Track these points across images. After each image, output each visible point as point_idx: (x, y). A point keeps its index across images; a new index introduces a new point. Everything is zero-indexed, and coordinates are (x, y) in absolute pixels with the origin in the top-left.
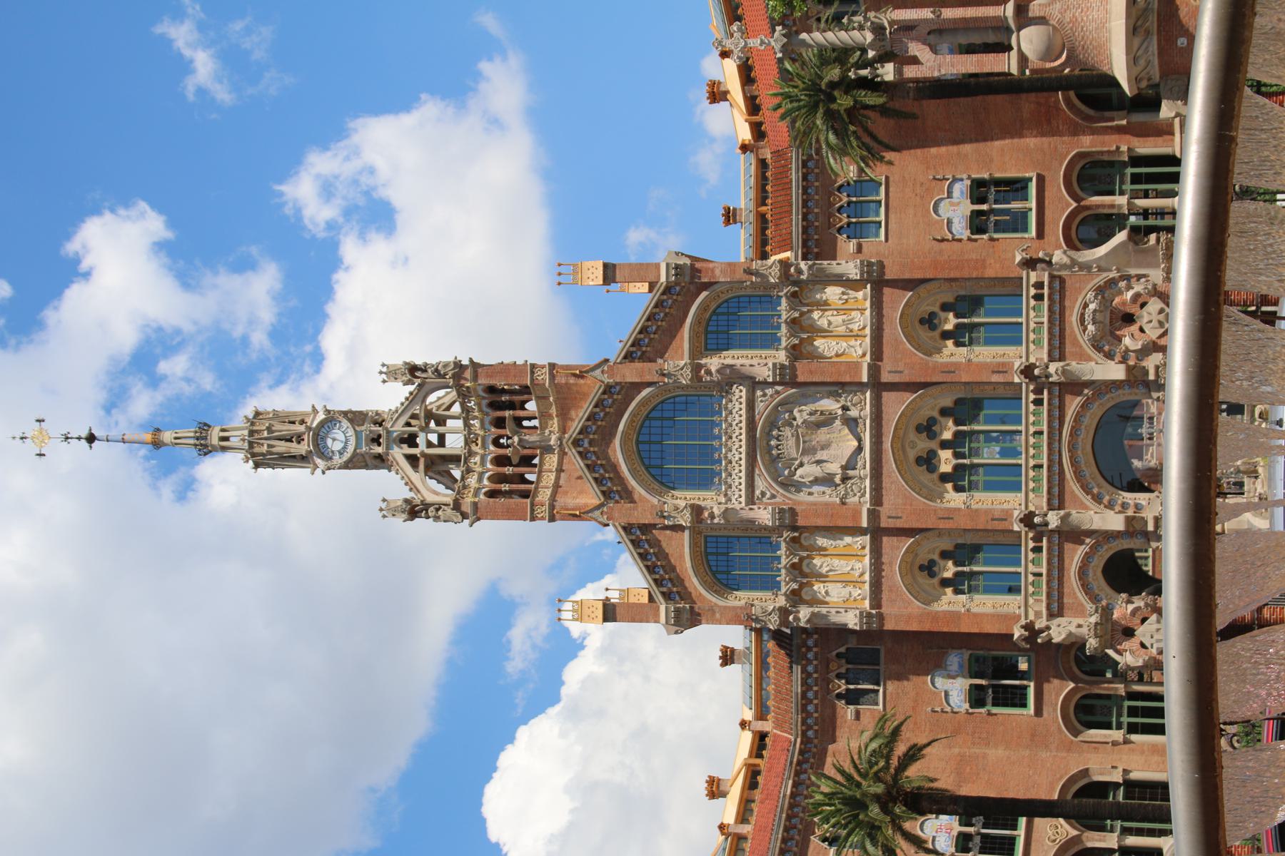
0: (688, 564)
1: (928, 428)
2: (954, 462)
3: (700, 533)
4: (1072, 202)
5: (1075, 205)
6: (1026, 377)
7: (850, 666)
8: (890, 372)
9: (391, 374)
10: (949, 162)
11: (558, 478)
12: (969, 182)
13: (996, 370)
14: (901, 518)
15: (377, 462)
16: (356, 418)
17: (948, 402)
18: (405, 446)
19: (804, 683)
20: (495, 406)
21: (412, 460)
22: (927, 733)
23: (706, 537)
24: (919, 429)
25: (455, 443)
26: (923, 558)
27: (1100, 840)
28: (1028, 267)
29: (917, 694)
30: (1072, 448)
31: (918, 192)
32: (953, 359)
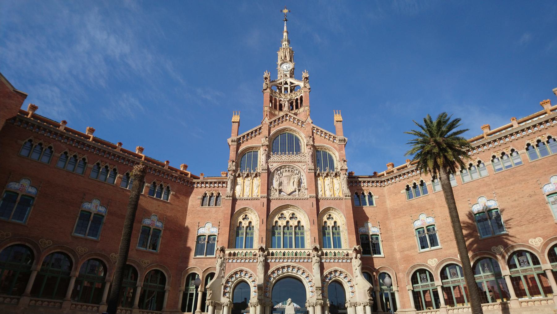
1: (293, 217)
3: (259, 149)
7: (215, 197)
8: (313, 203)
10: (384, 227)
13: (315, 238)
14: (263, 207)
17: (302, 223)
18: (285, 82)
20: (297, 99)
22: (191, 222)
23: (257, 151)
24: (293, 214)
26: (249, 216)
28: (354, 250)
29: (204, 218)
31: (372, 217)
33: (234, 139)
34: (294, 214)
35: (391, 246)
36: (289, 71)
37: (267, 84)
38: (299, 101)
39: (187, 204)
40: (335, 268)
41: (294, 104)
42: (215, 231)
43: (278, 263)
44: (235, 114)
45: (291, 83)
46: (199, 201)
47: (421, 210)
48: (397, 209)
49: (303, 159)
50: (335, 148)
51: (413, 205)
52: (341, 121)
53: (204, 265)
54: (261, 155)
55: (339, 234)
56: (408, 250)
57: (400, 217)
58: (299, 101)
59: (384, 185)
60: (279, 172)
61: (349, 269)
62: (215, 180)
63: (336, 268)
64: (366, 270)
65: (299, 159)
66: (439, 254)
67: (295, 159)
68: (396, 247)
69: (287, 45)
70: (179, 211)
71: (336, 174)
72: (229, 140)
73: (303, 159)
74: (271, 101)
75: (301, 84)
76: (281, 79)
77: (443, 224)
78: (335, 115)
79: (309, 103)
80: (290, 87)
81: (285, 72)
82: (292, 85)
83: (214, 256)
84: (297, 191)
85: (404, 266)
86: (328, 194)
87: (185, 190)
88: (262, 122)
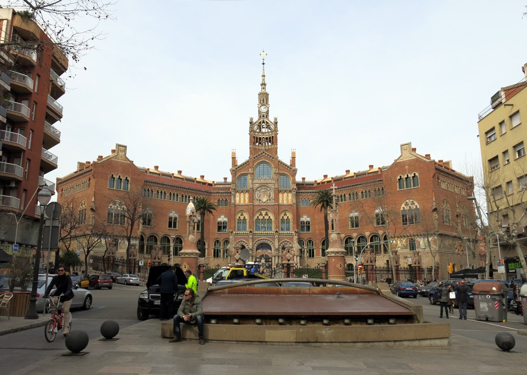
0: (242, 173)
1: (266, 214)
2: (261, 219)
9: (276, 119)
11: (257, 149)
15: (260, 116)
16: (267, 112)
17: (271, 218)
19: (222, 193)
20: (270, 137)
21: (260, 123)
24: (266, 213)
25: (263, 130)
26: (244, 214)
30: (264, 239)
58: (271, 140)
60: (259, 189)
68: (317, 228)
71: (290, 191)
81: (263, 114)
84: (269, 200)
86: (285, 202)
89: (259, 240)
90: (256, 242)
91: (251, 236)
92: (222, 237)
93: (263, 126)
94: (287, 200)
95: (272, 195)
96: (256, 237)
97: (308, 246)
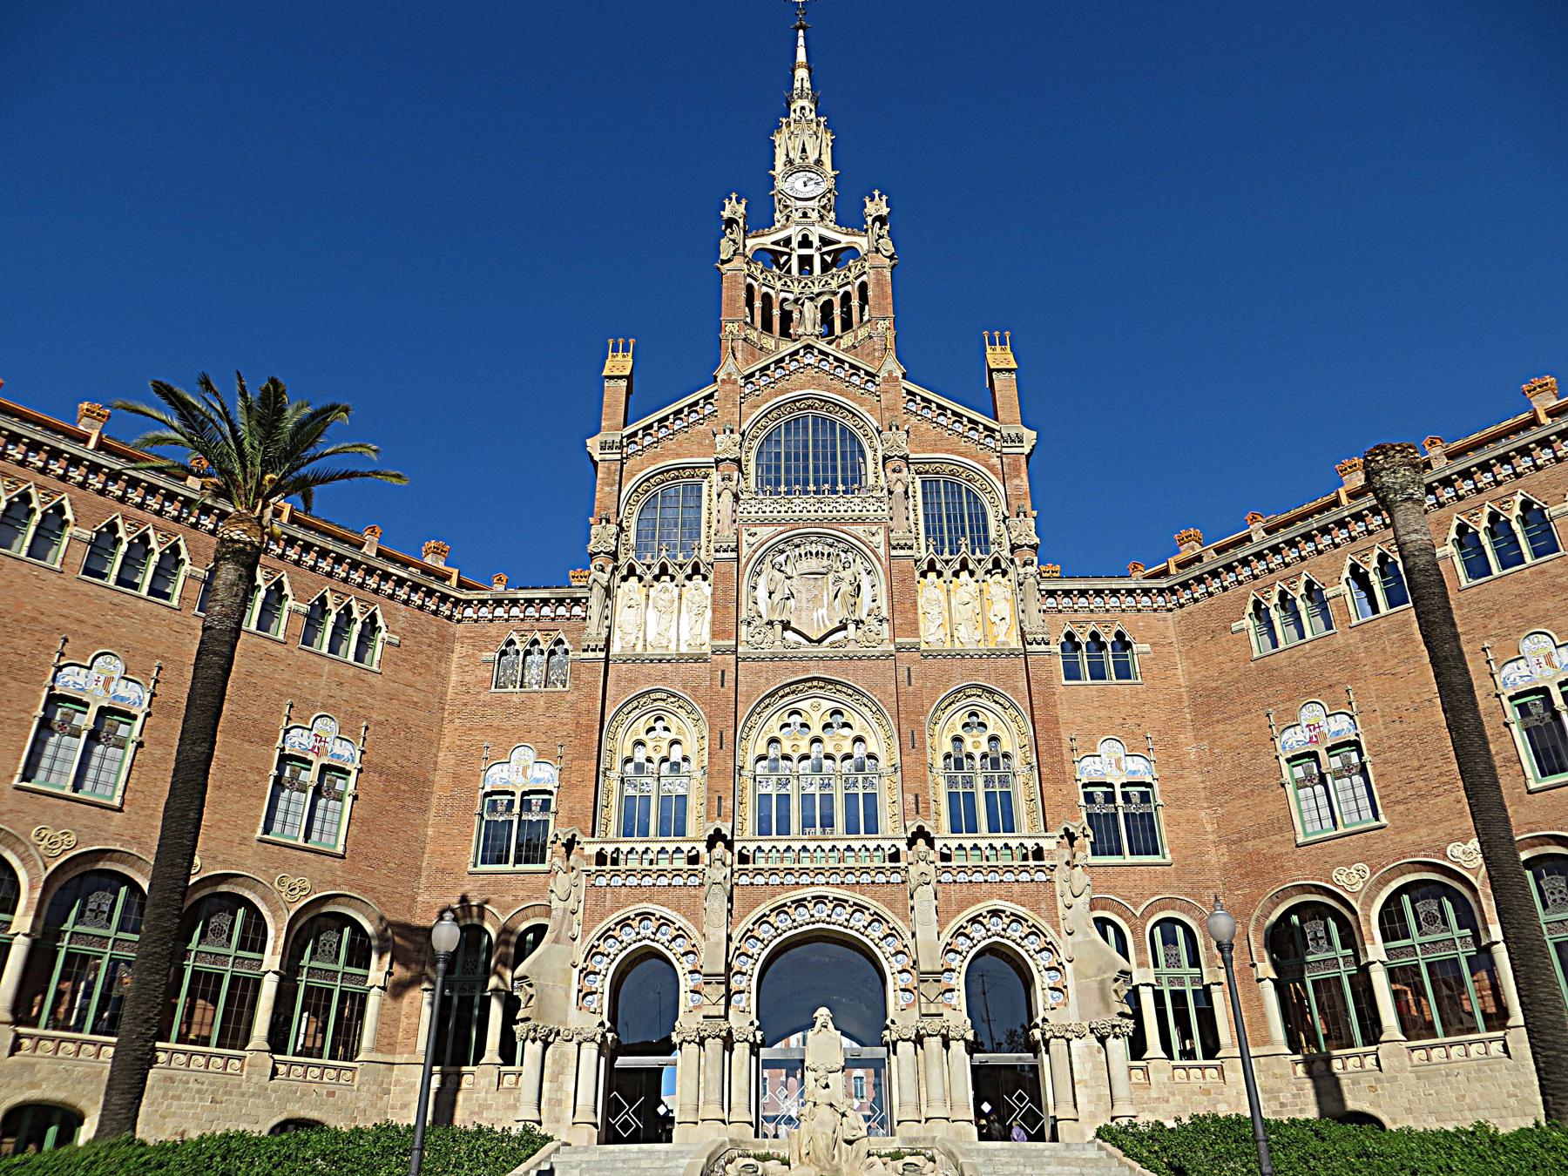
4: (1142, 908)
5: (1138, 914)
6: (913, 833)
12: (1148, 779)
14: (722, 685)
19: (530, 602)
20: (847, 297)
21: (787, 241)
22: (458, 743)
24: (836, 712)
27: (274, 948)
29: (507, 730)
30: (820, 899)
31: (1128, 721)
32: (929, 750)
33: (610, 439)
34: (842, 714)
35: (1195, 821)
36: (814, 198)
37: (734, 241)
38: (855, 303)
39: (444, 679)
40: (989, 903)
41: (837, 311)
42: (546, 776)
43: (778, 890)
44: (615, 350)
45: (825, 241)
46: (488, 671)
47: (1304, 687)
48: (1217, 688)
49: (872, 508)
50: (991, 468)
51: (1276, 673)
52: (1009, 370)
53: (510, 899)
54: (715, 497)
55: (1004, 781)
56: (1259, 836)
57: (1230, 718)
58: (855, 303)
59: (1169, 605)
61: (1043, 905)
62: (544, 594)
63: (996, 901)
64: (1104, 909)
65: (857, 508)
66: (1375, 846)
67: (842, 508)
68: (1209, 828)
69: (808, 110)
70: (416, 703)
71: (996, 564)
72: (593, 444)
73: (872, 508)
74: (750, 302)
75: (862, 243)
76: (784, 227)
77: (1389, 738)
78: (989, 350)
79: (890, 309)
80: (822, 254)
81: (799, 204)
82: (825, 249)
83: (545, 867)
84: (851, 627)
85: (1245, 895)
87: (435, 629)
88: (716, 377)
89: (780, 909)
90: (761, 920)
91: (719, 873)
92: (510, 899)
93: (800, 257)
94: (983, 620)
95: (874, 595)
96: (760, 880)
97: (1156, 965)
